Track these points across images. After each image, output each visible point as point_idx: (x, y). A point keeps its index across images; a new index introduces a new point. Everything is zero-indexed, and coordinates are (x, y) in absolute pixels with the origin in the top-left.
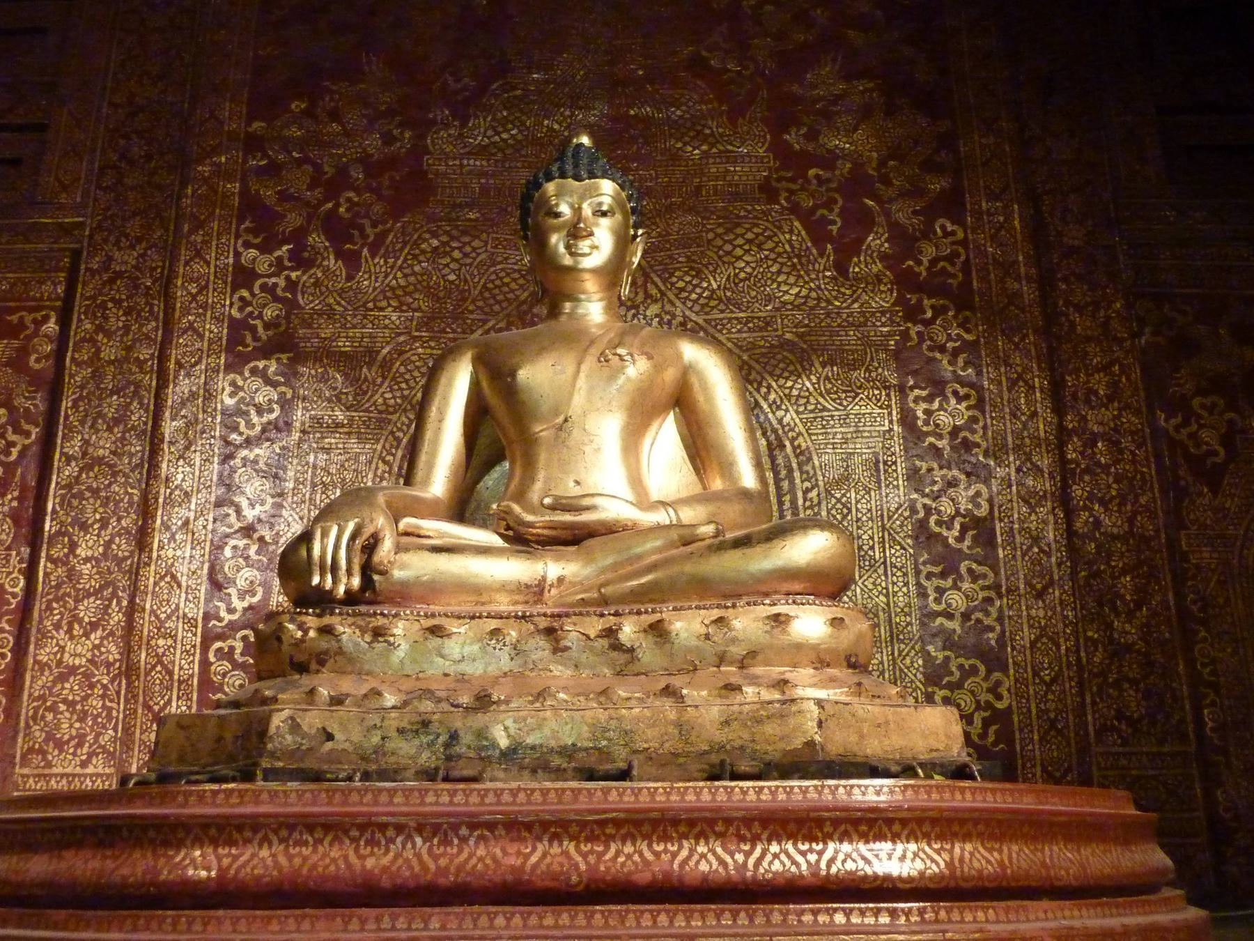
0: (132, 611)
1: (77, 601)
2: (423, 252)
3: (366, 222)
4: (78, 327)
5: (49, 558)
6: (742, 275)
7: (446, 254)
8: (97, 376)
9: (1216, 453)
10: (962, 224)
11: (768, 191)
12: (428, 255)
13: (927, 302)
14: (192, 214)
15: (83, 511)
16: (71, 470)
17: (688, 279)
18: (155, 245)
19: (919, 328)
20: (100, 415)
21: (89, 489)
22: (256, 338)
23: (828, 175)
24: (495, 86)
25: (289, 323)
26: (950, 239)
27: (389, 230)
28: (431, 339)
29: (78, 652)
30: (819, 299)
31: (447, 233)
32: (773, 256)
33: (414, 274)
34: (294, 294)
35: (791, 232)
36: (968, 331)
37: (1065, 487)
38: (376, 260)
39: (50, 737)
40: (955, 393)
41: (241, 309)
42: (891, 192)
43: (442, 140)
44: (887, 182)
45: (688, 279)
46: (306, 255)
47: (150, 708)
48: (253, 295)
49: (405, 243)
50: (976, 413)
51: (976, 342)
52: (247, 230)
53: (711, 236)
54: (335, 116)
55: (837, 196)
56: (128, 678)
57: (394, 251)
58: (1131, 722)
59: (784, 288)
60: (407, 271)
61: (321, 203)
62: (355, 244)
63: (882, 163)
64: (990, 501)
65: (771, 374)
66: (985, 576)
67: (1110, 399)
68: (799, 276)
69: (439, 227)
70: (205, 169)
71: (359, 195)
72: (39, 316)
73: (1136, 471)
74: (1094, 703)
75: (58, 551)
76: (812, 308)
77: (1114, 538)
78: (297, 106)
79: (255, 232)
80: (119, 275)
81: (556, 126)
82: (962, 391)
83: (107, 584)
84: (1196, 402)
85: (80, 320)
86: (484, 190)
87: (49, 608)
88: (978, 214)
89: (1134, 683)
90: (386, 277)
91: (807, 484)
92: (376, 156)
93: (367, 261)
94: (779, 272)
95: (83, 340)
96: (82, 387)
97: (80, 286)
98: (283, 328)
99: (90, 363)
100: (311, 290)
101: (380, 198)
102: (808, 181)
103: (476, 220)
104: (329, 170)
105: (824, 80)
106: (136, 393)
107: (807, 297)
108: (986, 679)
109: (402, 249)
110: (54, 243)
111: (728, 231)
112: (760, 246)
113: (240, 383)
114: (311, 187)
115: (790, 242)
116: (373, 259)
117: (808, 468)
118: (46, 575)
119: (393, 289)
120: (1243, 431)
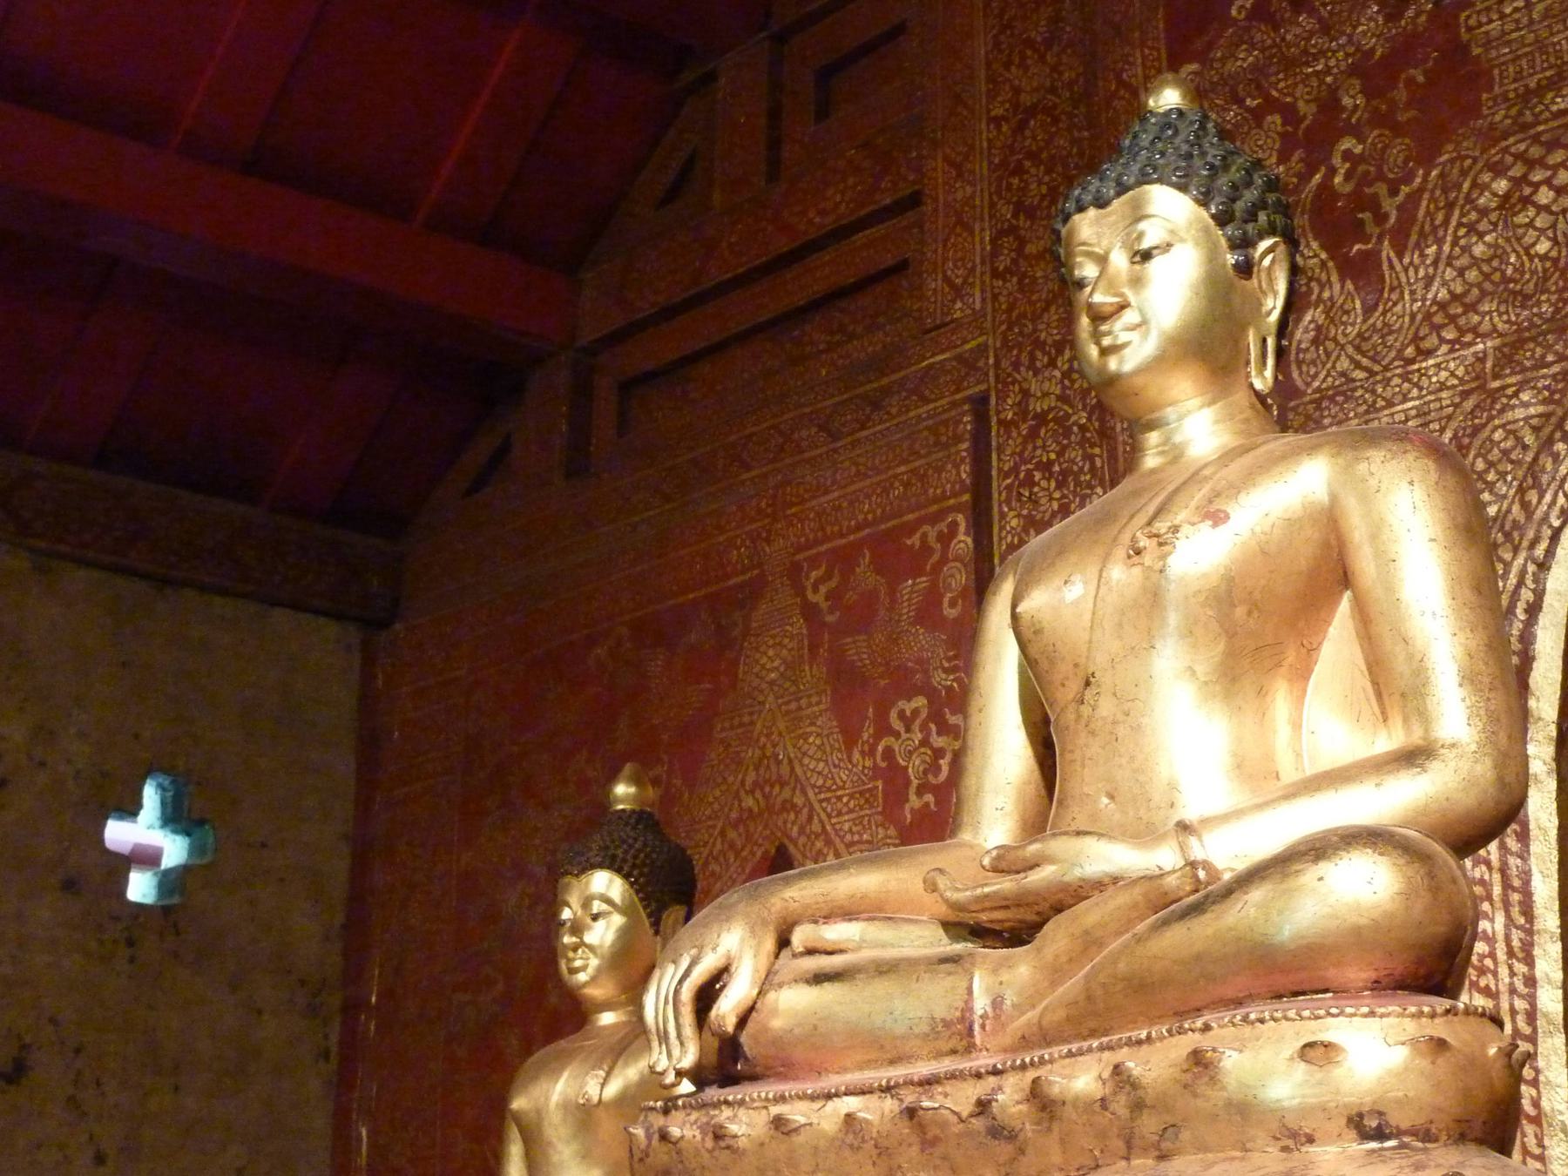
2: (1484, 212)
3: (1381, 189)
4: (1002, 528)
7: (1527, 201)
12: (1494, 216)
28: (1521, 387)
31: (1518, 157)
33: (1476, 262)
38: (1406, 260)
49: (1450, 206)
57: (1435, 229)
61: (1304, 178)
69: (1505, 150)
71: (1361, 139)
72: (943, 526)
90: (1427, 287)
92: (1378, 53)
93: (1392, 267)
97: (994, 456)
101: (1397, 130)
104: (1307, 109)
109: (1446, 222)
110: (958, 390)
116: (1400, 256)
119: (1443, 306)
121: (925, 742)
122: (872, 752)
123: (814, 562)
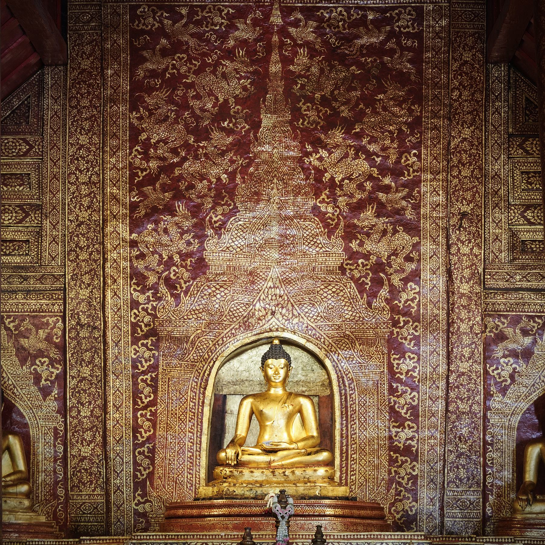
0: (104, 437)
2: (205, 295)
5: (70, 416)
6: (330, 307)
7: (215, 296)
8: (79, 343)
9: (506, 381)
11: (342, 270)
13: (402, 319)
14: (111, 276)
15: (81, 398)
16: (74, 382)
17: (309, 308)
18: (95, 287)
19: (398, 330)
20: (83, 360)
21: (82, 389)
22: (142, 331)
23: (367, 262)
24: (231, 220)
25: (154, 324)
26: (413, 291)
27: (192, 285)
28: (210, 332)
29: (86, 451)
30: (360, 317)
31: (214, 286)
32: (343, 299)
33: (202, 304)
34: (155, 312)
35: (350, 288)
36: (416, 331)
37: (447, 393)
39: (80, 481)
40: (409, 357)
41: (135, 318)
42: (391, 271)
43: (211, 245)
45: (309, 308)
46: (159, 295)
47: (116, 472)
48: (139, 312)
49: (198, 291)
50: (416, 364)
51: (419, 336)
52: (134, 284)
53: (319, 289)
55: (369, 272)
56: (106, 461)
58: (461, 480)
59: (346, 312)
60: (200, 303)
61: (163, 272)
62: (178, 291)
63: (389, 257)
64: (418, 399)
65: (340, 348)
66: (413, 427)
68: (353, 307)
70: (115, 255)
71: (178, 269)
73: (476, 387)
74: (448, 473)
75: (74, 414)
76: (357, 321)
77: (464, 413)
78: (150, 226)
79: (138, 284)
80: (83, 300)
81: (257, 238)
83: (94, 426)
84: (502, 360)
85: (69, 320)
86: (229, 267)
87: (73, 435)
91: (351, 392)
94: (345, 306)
95: (72, 328)
96: (74, 348)
98: (152, 326)
99: (75, 338)
100: (162, 310)
101: (187, 270)
102: (359, 265)
103: (226, 281)
105: (368, 218)
106: (95, 351)
107: (355, 316)
108: (410, 464)
109: (197, 294)
111: (326, 287)
112: (337, 294)
113: (138, 349)
114: (159, 265)
115: (349, 292)
117: (352, 386)
118: (70, 423)
119: (194, 310)
120: (518, 372)
122: (30, 368)
123: (9, 317)
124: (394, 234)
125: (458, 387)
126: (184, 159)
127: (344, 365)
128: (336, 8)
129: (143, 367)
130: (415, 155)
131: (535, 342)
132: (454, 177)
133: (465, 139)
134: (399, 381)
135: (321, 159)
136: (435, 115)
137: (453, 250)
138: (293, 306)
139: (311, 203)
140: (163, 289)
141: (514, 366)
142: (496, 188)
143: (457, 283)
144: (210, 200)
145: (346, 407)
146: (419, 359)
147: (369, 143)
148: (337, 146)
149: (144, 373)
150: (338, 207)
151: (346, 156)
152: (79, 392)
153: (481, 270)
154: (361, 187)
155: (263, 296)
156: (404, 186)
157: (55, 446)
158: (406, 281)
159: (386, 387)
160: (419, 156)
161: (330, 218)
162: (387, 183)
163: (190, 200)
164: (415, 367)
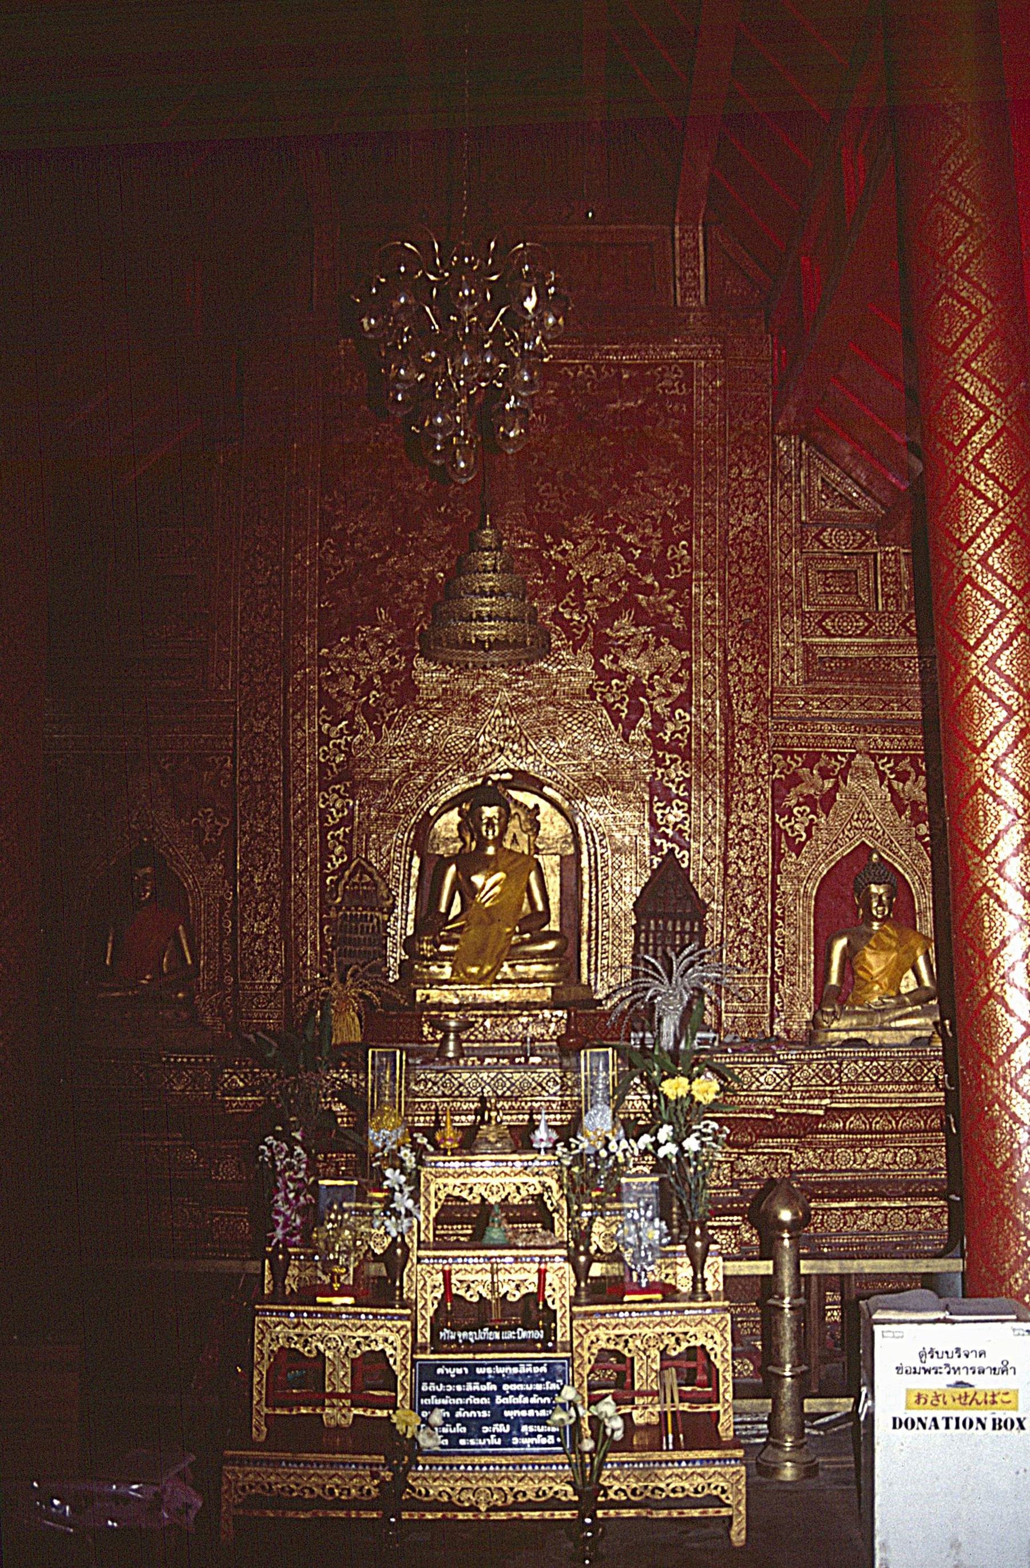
1: (257, 904)
8: (254, 790)
10: (690, 713)
22: (333, 773)
37: (726, 851)
44: (653, 689)
54: (364, 646)
61: (361, 697)
63: (651, 677)
67: (754, 807)
82: (681, 804)
84: (795, 811)
86: (445, 690)
88: (698, 707)
89: (746, 946)
105: (624, 626)
114: (355, 689)
121: (212, 822)
124: (656, 648)
125: (739, 844)
126: (388, 555)
127: (594, 815)
128: (583, 365)
129: (334, 819)
130: (684, 547)
131: (836, 787)
132: (732, 575)
133: (747, 528)
134: (665, 836)
135: (564, 552)
136: (709, 498)
137: (733, 668)
138: (527, 741)
139: (551, 608)
140: (360, 719)
141: (811, 816)
142: (787, 589)
143: (737, 710)
144: (421, 605)
145: (596, 870)
146: (690, 808)
147: (625, 531)
148: (584, 536)
149: (336, 827)
150: (586, 613)
151: (597, 547)
152: (252, 851)
153: (768, 694)
154: (615, 588)
155: (489, 728)
156: (671, 584)
157: (221, 921)
158: (673, 707)
159: (647, 843)
160: (689, 549)
161: (575, 626)
162: (649, 581)
163: (398, 606)
164: (685, 819)
